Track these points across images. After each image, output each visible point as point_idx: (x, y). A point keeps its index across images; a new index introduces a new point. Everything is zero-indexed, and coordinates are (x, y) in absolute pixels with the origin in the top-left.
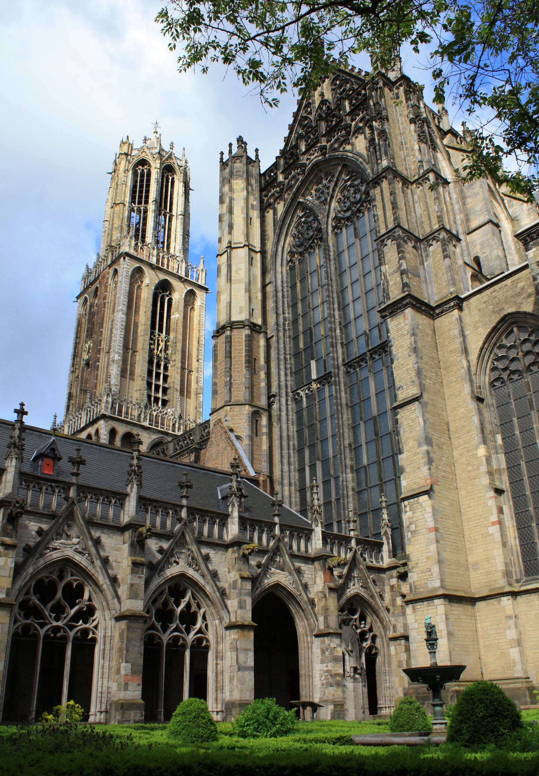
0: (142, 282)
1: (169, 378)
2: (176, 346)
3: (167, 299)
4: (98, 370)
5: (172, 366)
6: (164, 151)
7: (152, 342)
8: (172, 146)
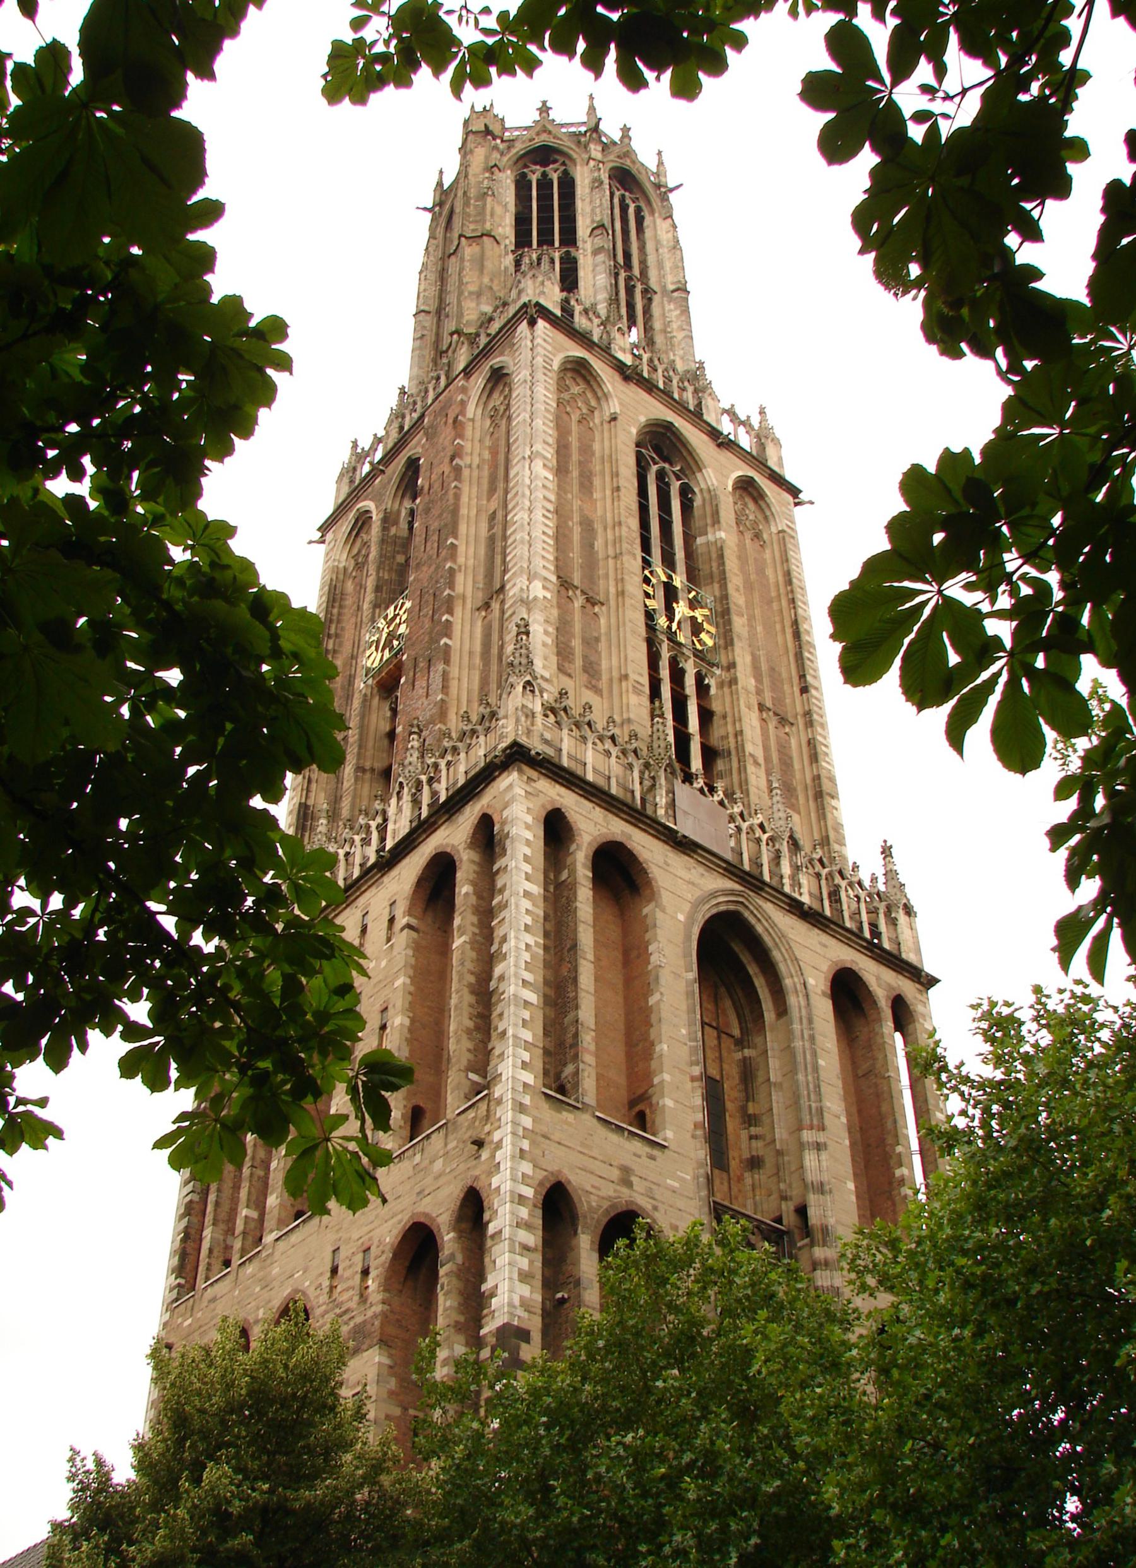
2: (729, 622)
3: (675, 486)
4: (447, 661)
5: (721, 685)
8: (626, 130)
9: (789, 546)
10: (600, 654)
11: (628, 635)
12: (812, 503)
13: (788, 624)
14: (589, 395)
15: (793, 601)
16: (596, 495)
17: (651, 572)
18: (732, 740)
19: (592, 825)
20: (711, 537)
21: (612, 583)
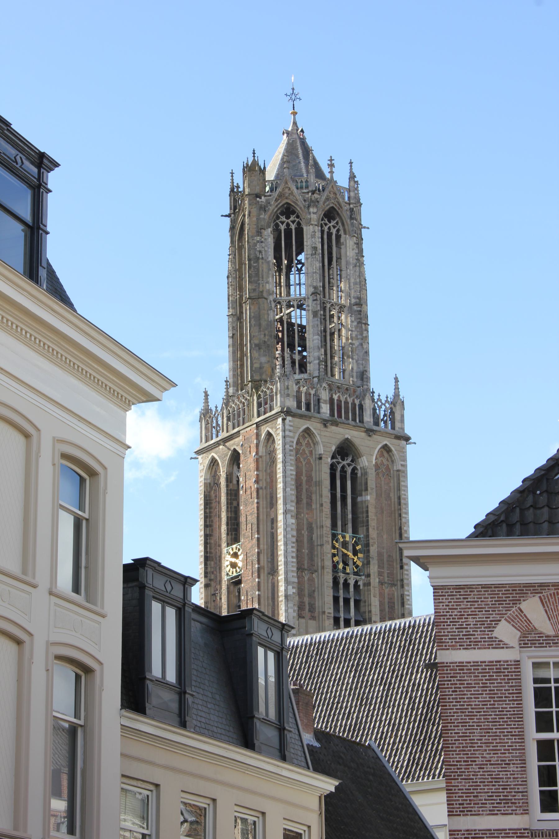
1: (362, 604)
2: (368, 551)
3: (349, 470)
5: (364, 585)
10: (314, 598)
11: (325, 590)
12: (415, 443)
13: (397, 528)
15: (400, 515)
18: (367, 614)
20: (363, 498)
21: (319, 560)
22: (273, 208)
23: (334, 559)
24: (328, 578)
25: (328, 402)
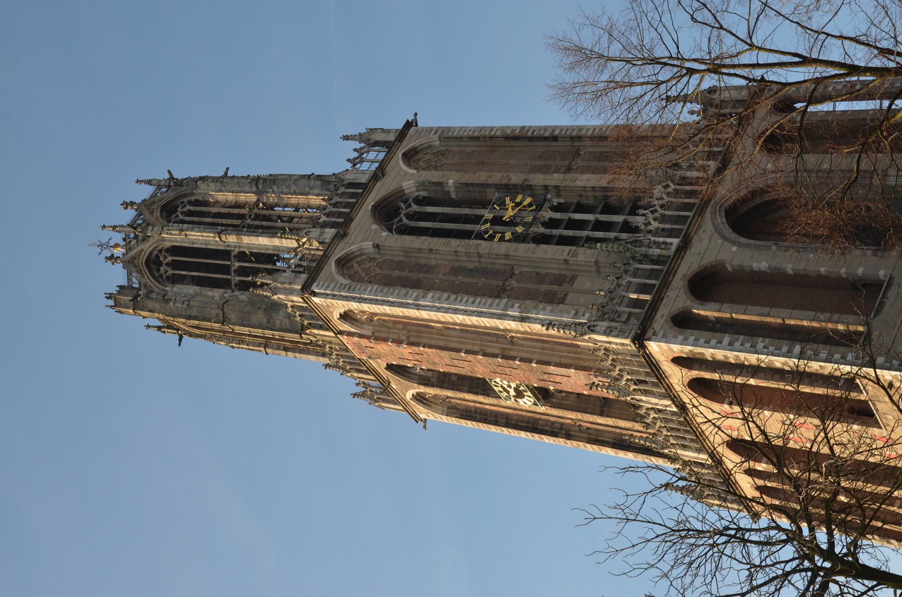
0: (371, 259)
2: (515, 186)
3: (415, 207)
5: (558, 196)
6: (134, 220)
7: (498, 236)
8: (126, 205)
9: (450, 134)
10: (547, 274)
11: (536, 256)
12: (416, 114)
13: (507, 143)
14: (359, 259)
15: (491, 138)
16: (433, 263)
17: (486, 232)
18: (597, 194)
19: (677, 298)
20: (452, 189)
21: (498, 261)
22: (149, 280)
23: (507, 238)
24: (523, 249)
25: (322, 230)
